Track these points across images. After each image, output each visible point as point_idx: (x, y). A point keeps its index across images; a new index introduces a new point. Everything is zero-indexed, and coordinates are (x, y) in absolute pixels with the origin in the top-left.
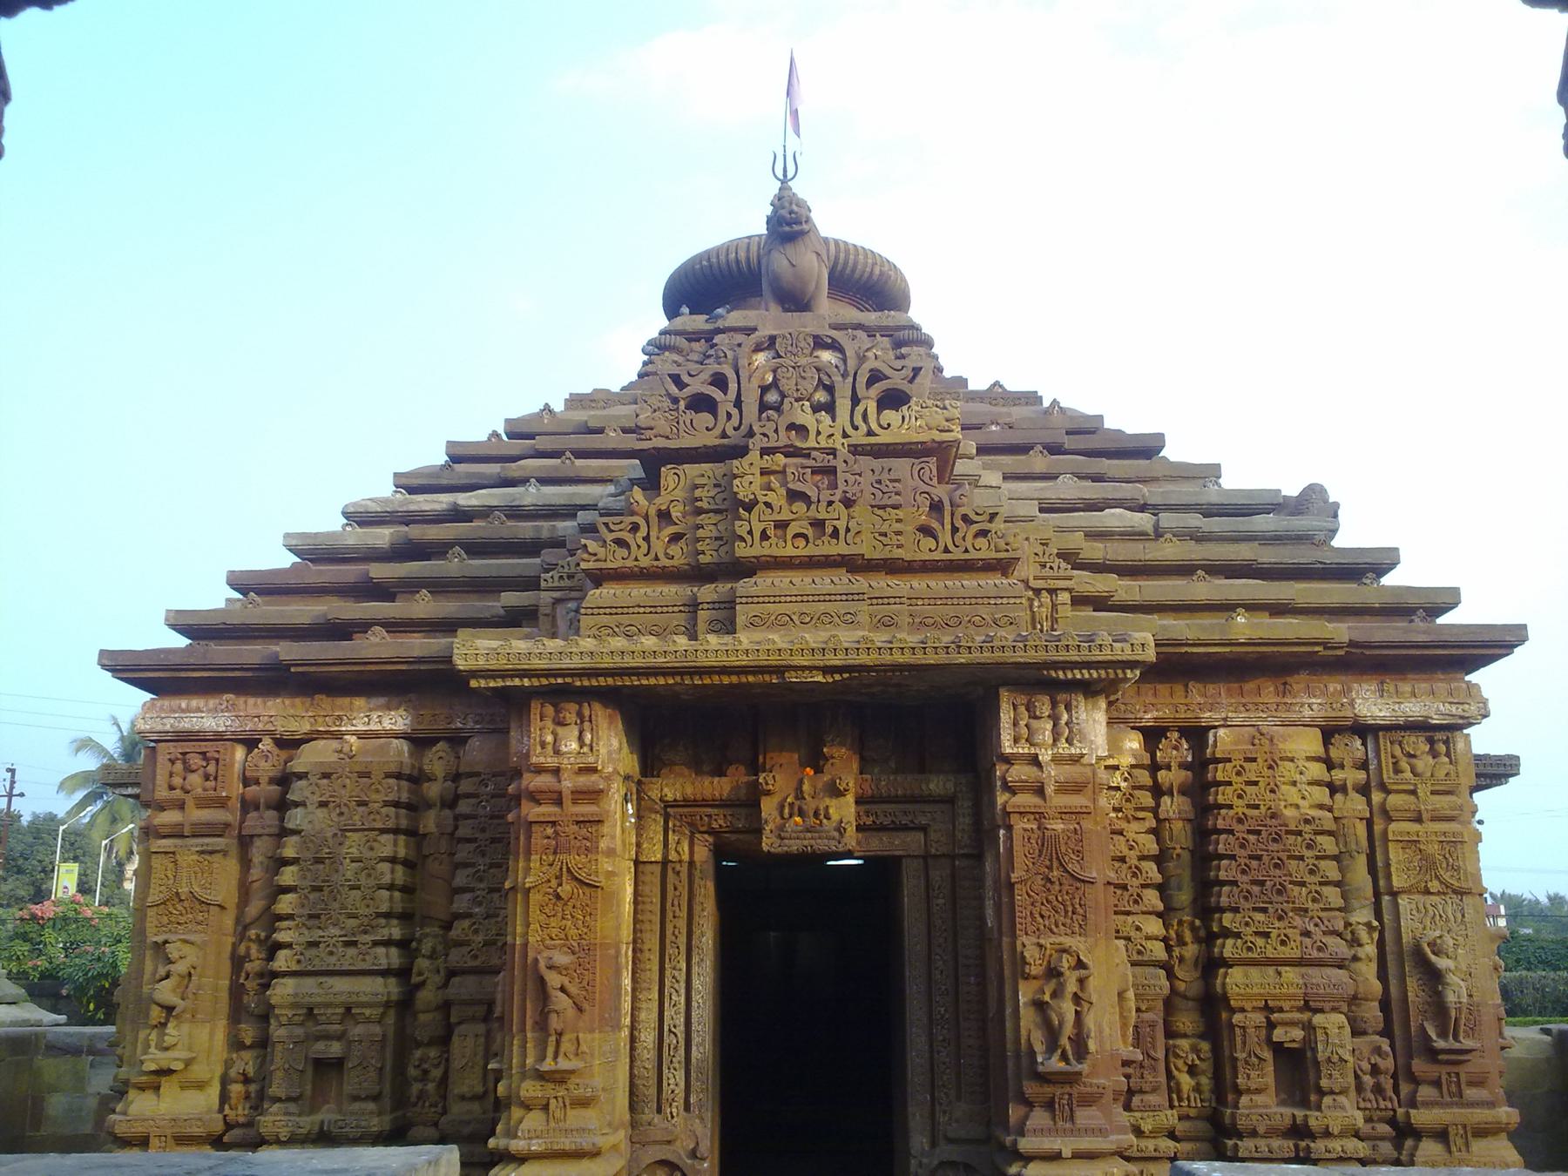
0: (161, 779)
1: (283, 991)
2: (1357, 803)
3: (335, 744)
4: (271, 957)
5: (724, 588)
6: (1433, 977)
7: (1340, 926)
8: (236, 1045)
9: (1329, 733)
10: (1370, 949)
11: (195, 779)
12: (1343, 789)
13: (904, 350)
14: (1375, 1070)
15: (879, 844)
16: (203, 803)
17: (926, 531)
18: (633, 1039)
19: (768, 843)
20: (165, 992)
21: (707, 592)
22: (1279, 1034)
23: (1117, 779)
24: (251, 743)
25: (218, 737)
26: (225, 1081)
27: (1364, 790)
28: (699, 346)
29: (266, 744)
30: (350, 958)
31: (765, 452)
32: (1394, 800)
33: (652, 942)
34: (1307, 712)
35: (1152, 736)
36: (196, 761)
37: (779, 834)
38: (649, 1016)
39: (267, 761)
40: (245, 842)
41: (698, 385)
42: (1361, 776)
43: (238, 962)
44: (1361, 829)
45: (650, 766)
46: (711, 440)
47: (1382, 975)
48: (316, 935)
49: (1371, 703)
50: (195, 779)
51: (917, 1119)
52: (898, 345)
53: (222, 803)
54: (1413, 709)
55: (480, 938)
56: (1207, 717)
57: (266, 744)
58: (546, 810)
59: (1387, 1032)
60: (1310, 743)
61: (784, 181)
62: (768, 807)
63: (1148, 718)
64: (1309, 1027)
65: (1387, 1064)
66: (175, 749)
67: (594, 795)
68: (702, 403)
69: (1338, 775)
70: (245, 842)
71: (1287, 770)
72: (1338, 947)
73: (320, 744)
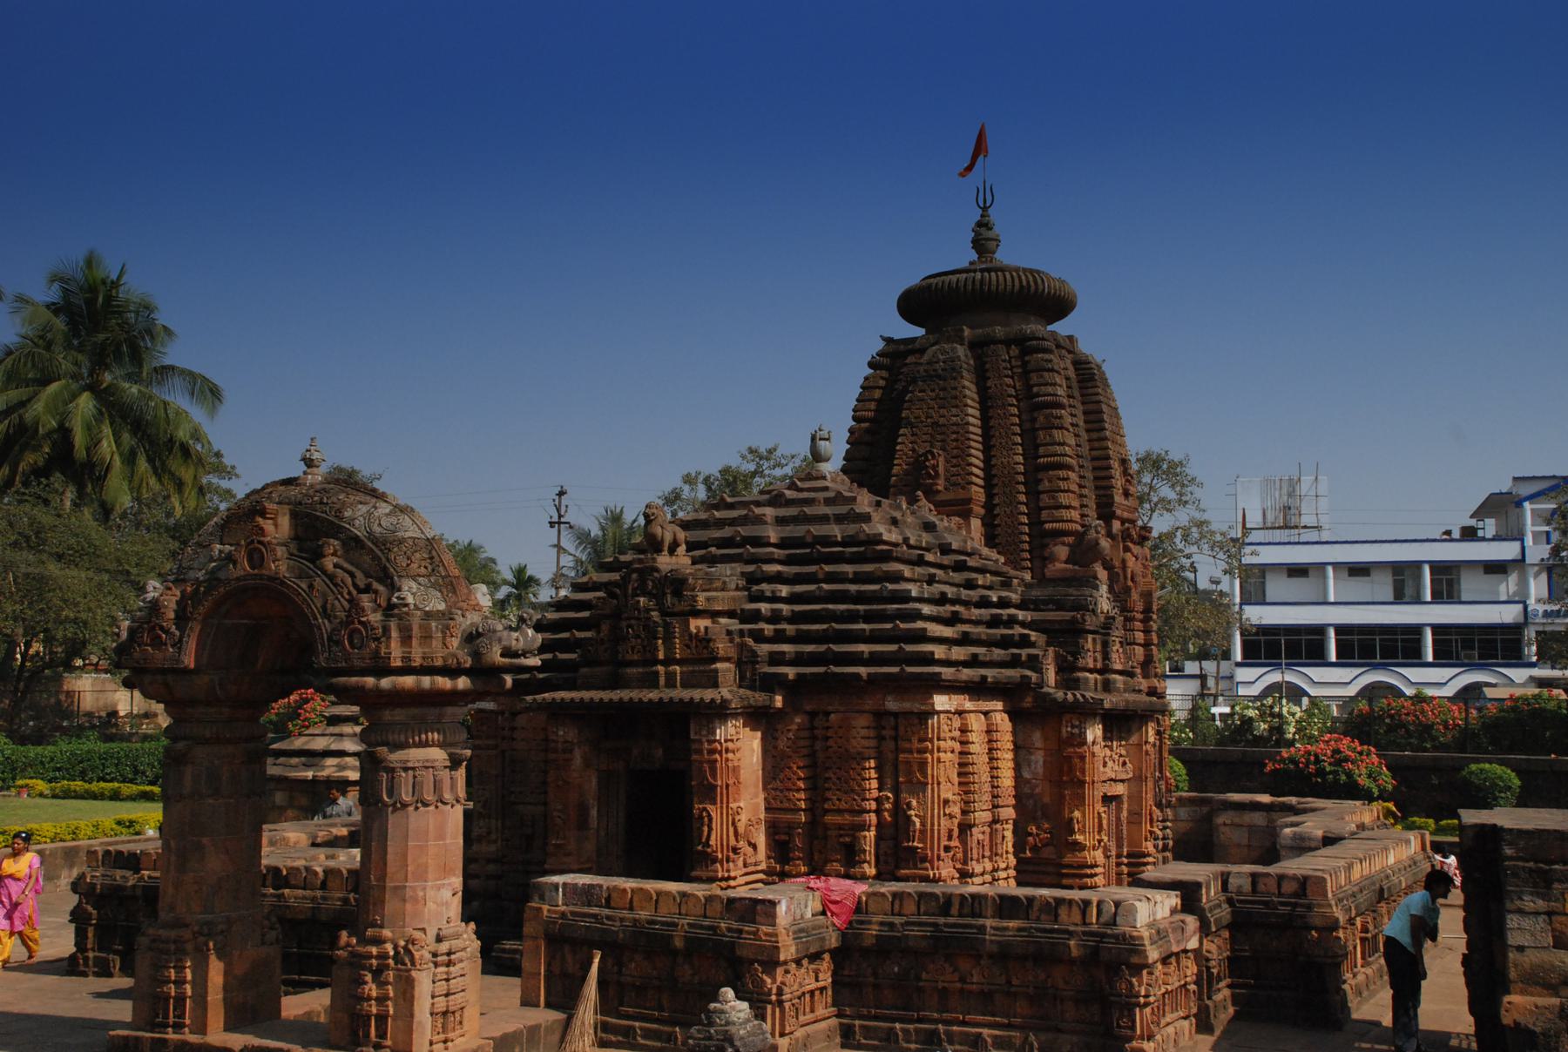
12: (883, 738)
17: (688, 646)
23: (791, 735)
24: (502, 713)
27: (895, 739)
34: (867, 707)
35: (812, 715)
42: (892, 733)
44: (891, 756)
49: (892, 705)
54: (907, 706)
56: (830, 708)
61: (985, 209)
63: (808, 708)
67: (571, 751)
71: (854, 732)
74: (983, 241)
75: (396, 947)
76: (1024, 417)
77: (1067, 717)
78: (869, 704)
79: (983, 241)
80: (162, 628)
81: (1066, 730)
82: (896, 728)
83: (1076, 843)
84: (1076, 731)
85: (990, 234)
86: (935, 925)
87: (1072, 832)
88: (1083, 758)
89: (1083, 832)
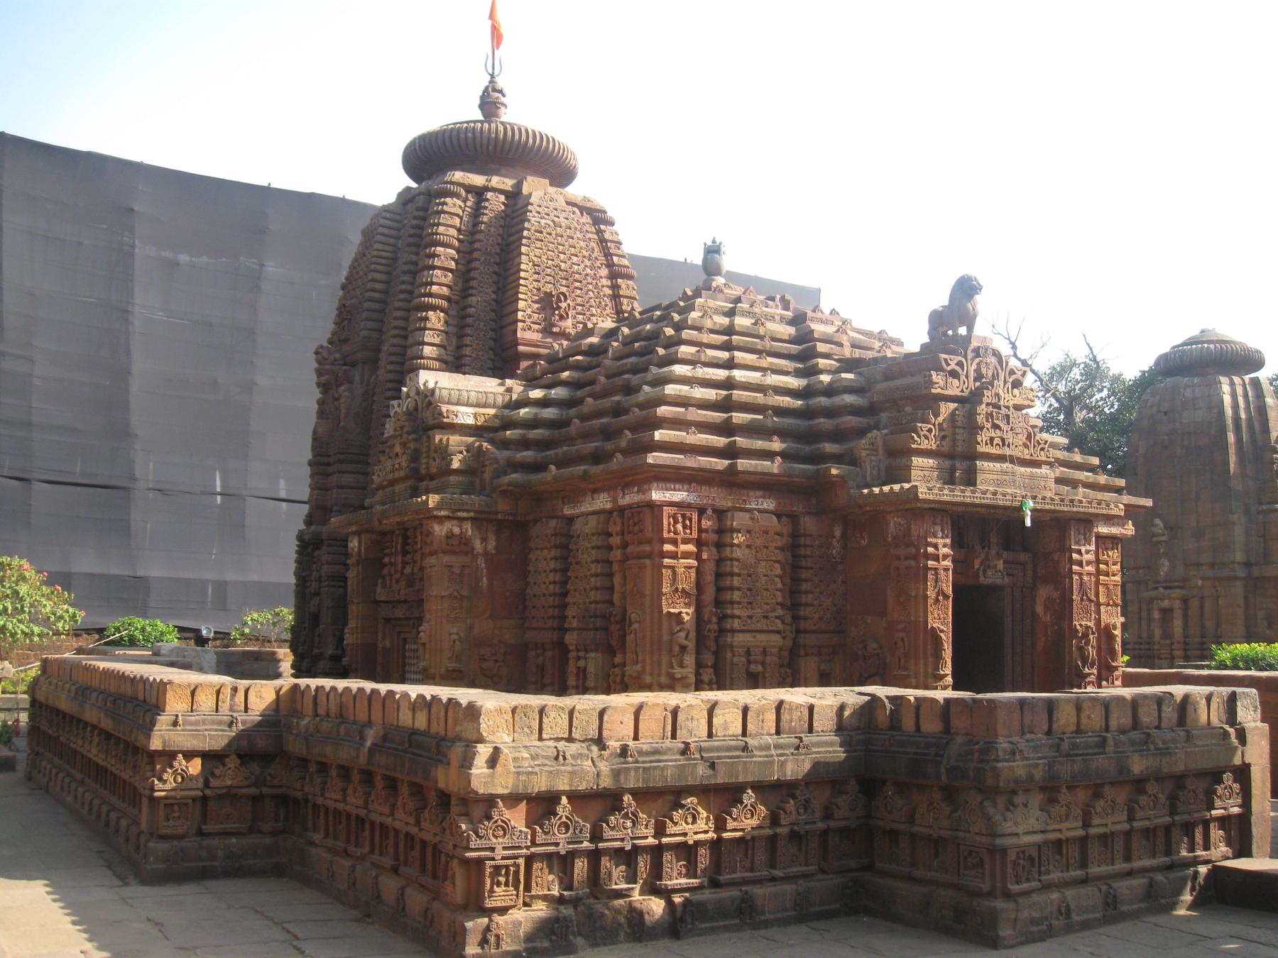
3: (747, 515)
16: (685, 542)
21: (960, 465)
24: (701, 511)
29: (709, 512)
30: (762, 625)
31: (988, 404)
41: (953, 366)
46: (957, 392)
48: (750, 612)
50: (679, 526)
55: (816, 616)
57: (709, 512)
58: (931, 563)
61: (492, 76)
66: (672, 510)
68: (954, 374)
74: (490, 103)
79: (490, 103)
85: (503, 100)
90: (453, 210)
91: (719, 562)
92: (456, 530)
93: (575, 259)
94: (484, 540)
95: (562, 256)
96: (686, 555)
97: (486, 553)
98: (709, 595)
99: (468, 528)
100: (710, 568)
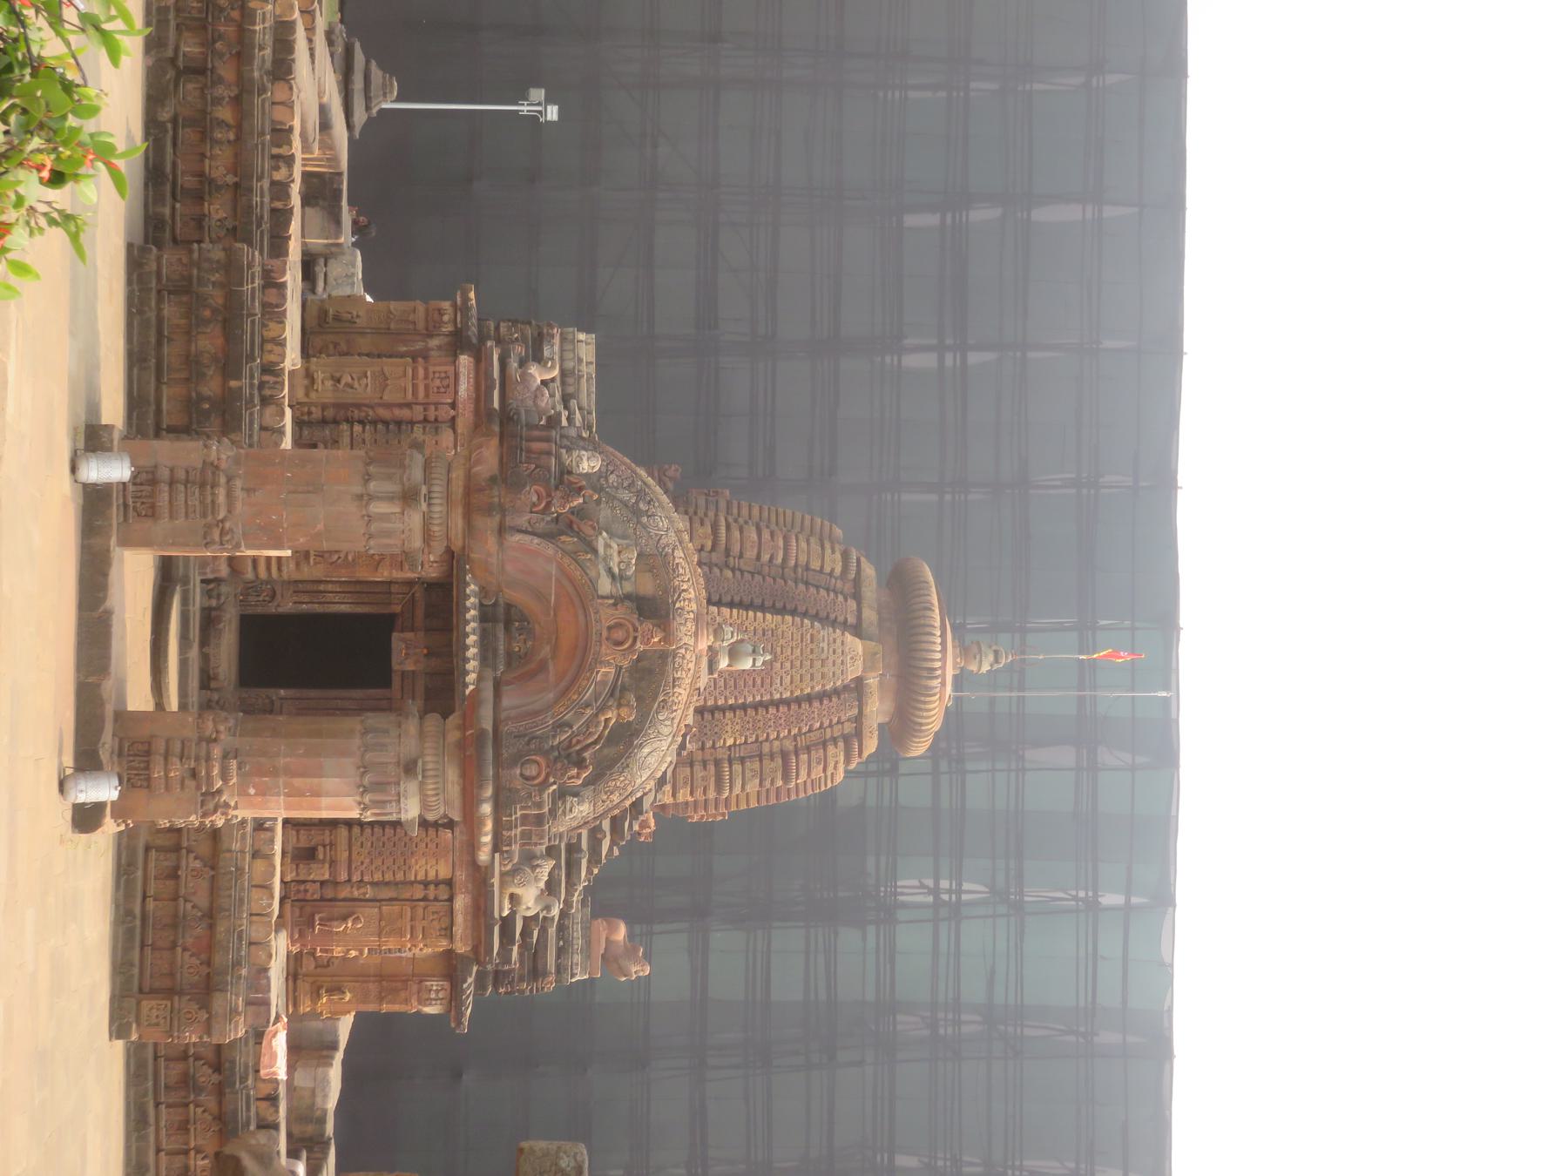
0: (438, 369)
1: (345, 426)
2: (419, 894)
3: (451, 445)
4: (360, 422)
5: (502, 617)
6: (344, 918)
7: (366, 879)
8: (324, 407)
9: (449, 883)
10: (356, 894)
11: (437, 382)
13: (841, 744)
14: (306, 891)
15: (396, 680)
16: (427, 387)
18: (321, 582)
19: (395, 635)
20: (347, 379)
22: (320, 849)
24: (453, 405)
25: (456, 392)
26: (310, 404)
27: (424, 899)
28: (848, 588)
29: (452, 413)
32: (420, 911)
33: (358, 588)
34: (458, 873)
36: (445, 382)
37: (398, 642)
38: (330, 587)
39: (445, 413)
40: (409, 405)
43: (358, 406)
44: (407, 895)
45: (430, 586)
47: (344, 900)
49: (461, 902)
50: (437, 382)
51: (291, 693)
52: (847, 739)
53: (427, 395)
54: (459, 919)
57: (452, 413)
59: (322, 899)
60: (444, 872)
62: (409, 635)
64: (323, 861)
65: (308, 897)
69: (432, 887)
70: (409, 405)
72: (355, 878)
73: (452, 438)
75: (219, 792)
76: (776, 743)
77: (446, 984)
78: (461, 876)
80: (548, 505)
81: (434, 985)
82: (436, 899)
83: (319, 997)
84: (433, 995)
86: (248, 1123)
87: (330, 991)
88: (406, 1001)
89: (329, 1000)
90: (827, 559)
91: (412, 423)
92: (446, 318)
93: (787, 680)
94: (439, 348)
95: (788, 665)
96: (415, 393)
97: (429, 349)
98: (383, 413)
99: (449, 328)
100: (405, 414)
